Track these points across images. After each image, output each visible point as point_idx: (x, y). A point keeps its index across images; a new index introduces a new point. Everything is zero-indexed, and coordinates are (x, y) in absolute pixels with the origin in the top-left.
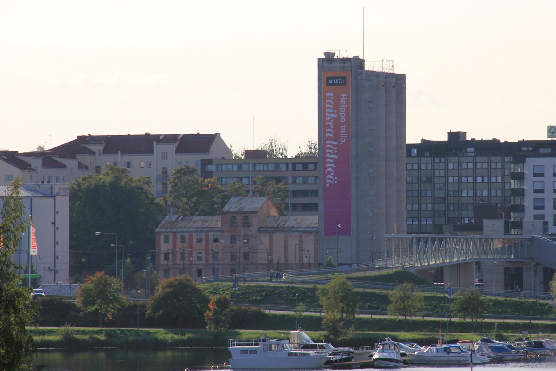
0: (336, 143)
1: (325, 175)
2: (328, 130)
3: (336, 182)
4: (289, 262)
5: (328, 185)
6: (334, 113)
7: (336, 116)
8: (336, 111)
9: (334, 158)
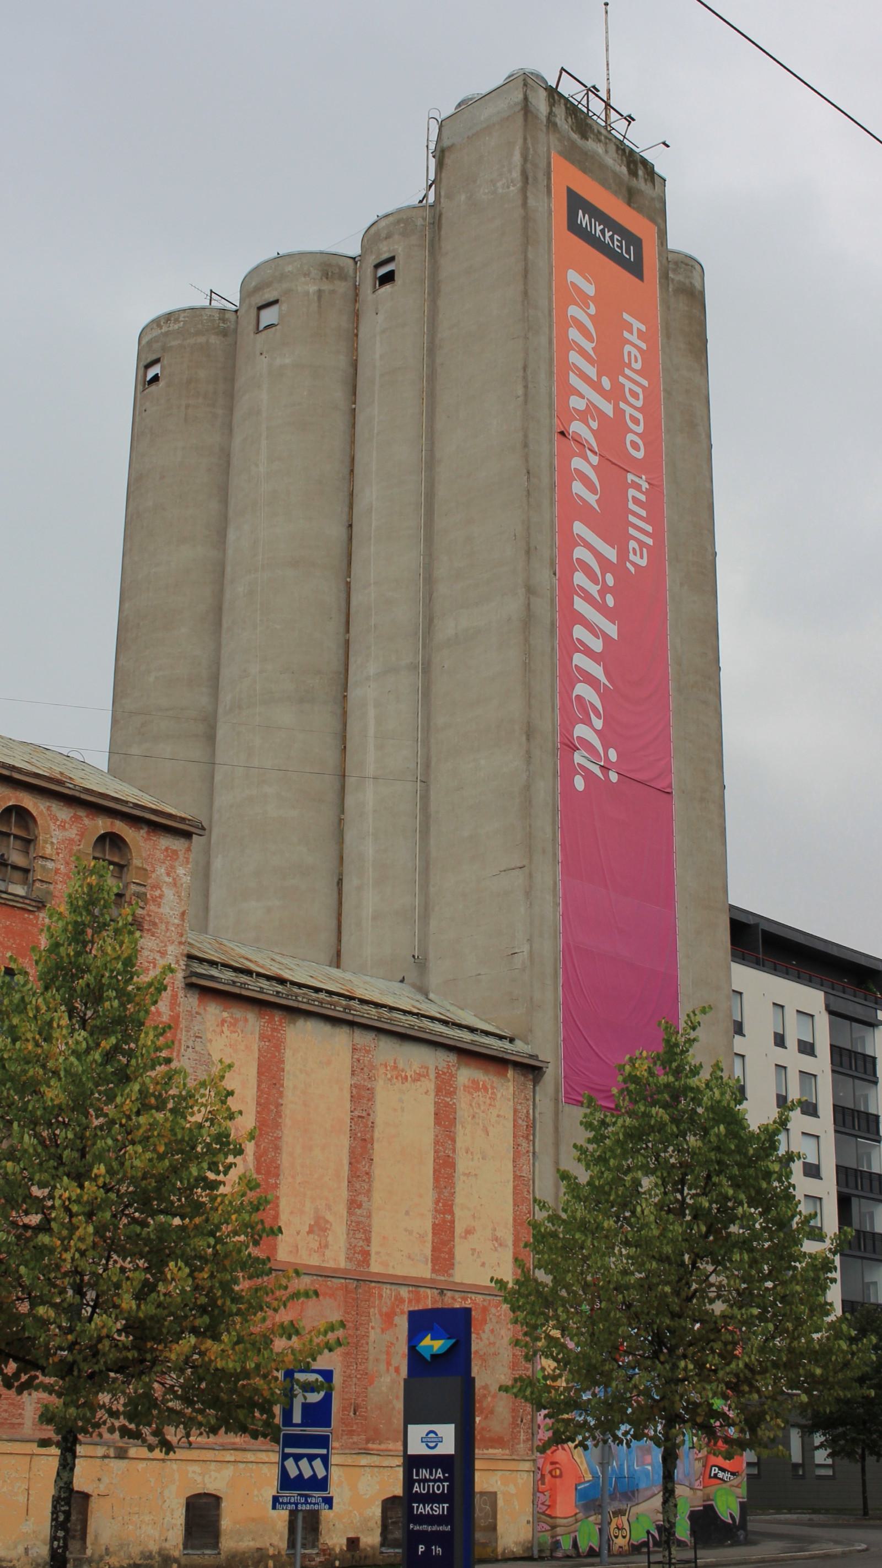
0: (611, 554)
1: (569, 722)
2: (577, 463)
3: (614, 777)
4: (375, 1267)
5: (579, 784)
6: (596, 386)
7: (608, 409)
8: (606, 383)
9: (606, 637)
